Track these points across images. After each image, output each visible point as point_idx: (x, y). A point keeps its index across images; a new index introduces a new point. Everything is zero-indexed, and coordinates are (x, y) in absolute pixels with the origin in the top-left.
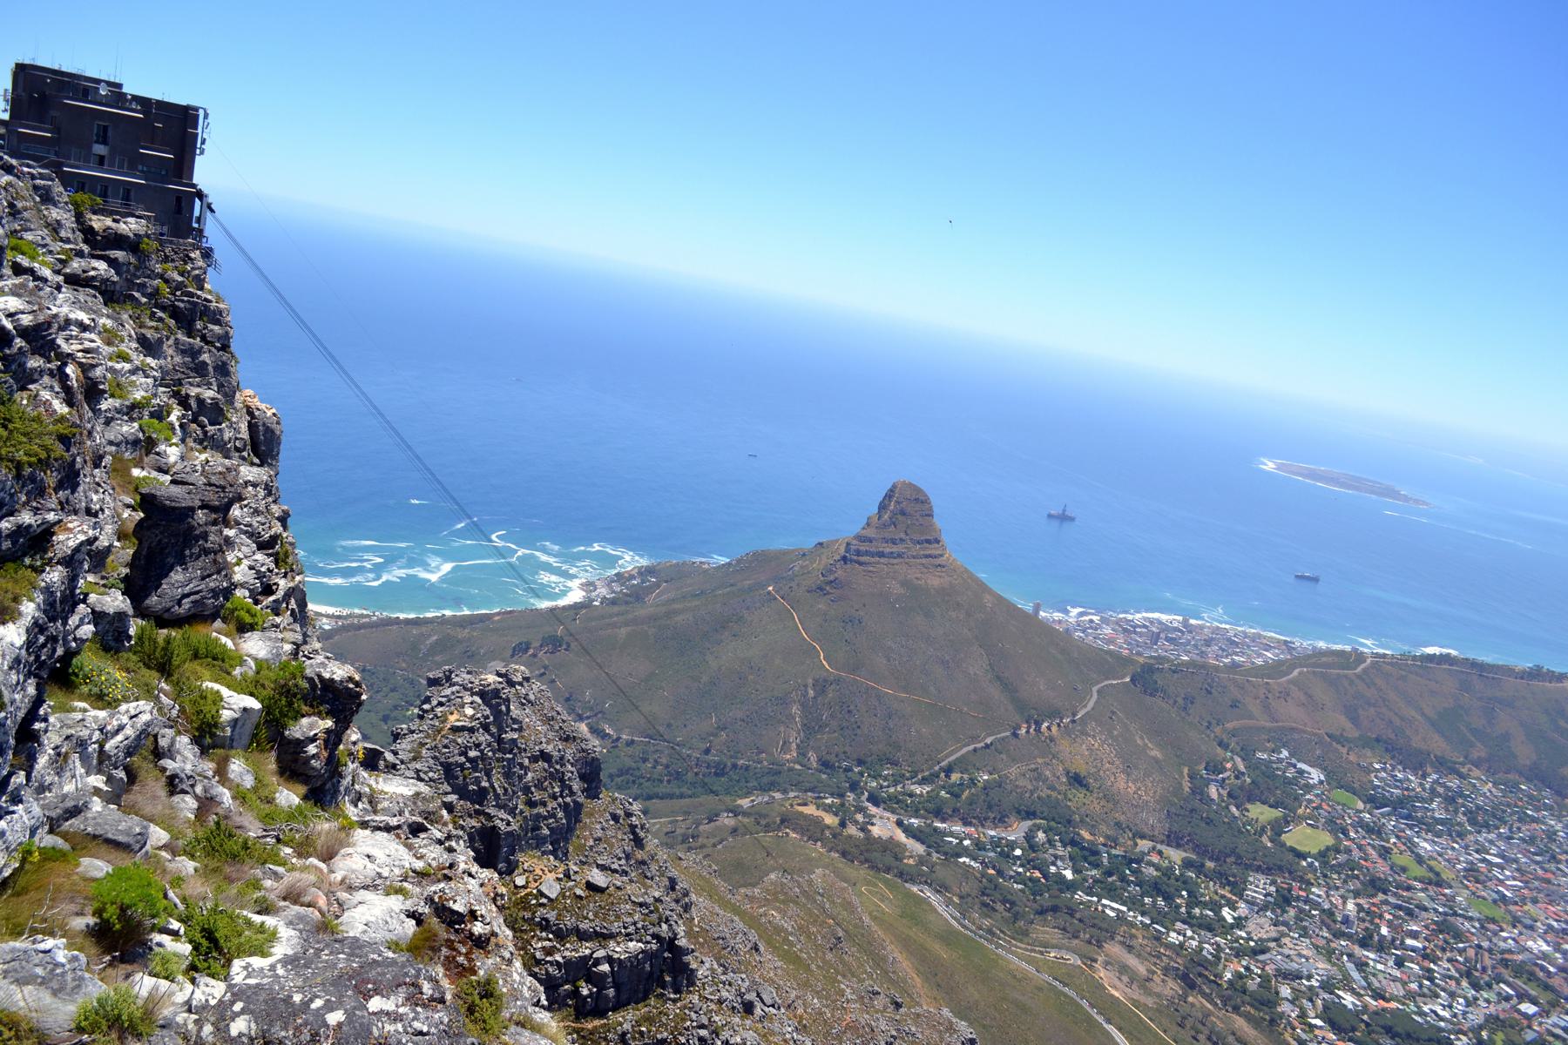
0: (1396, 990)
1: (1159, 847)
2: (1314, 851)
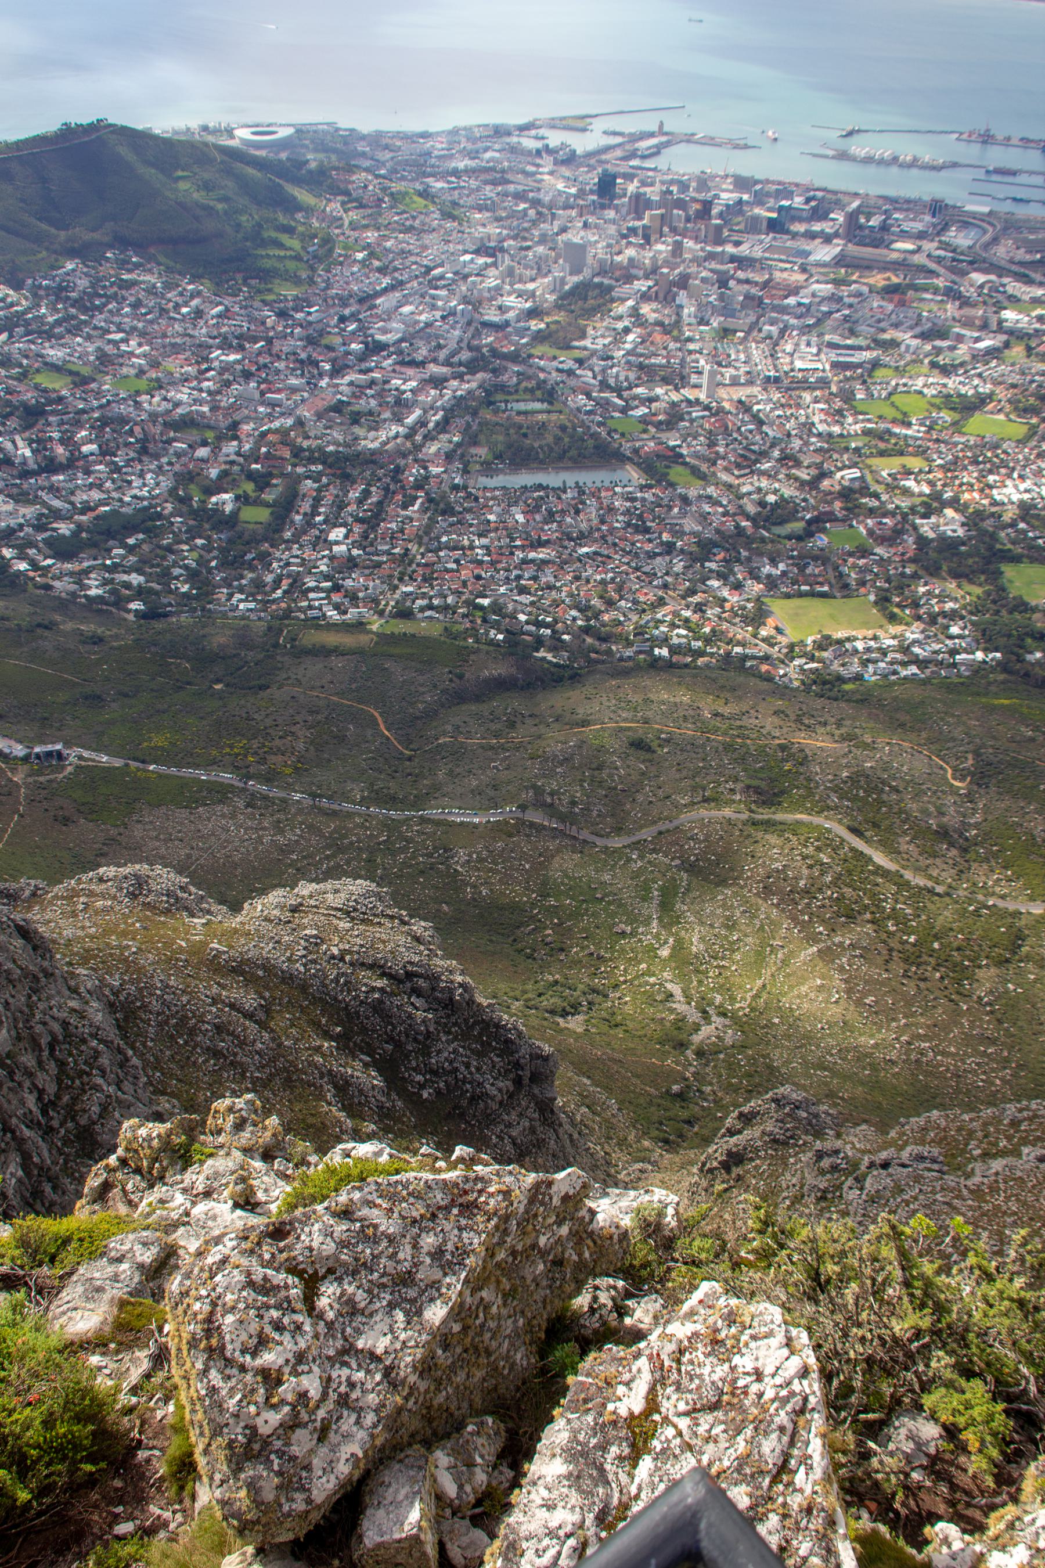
0: (96, 495)
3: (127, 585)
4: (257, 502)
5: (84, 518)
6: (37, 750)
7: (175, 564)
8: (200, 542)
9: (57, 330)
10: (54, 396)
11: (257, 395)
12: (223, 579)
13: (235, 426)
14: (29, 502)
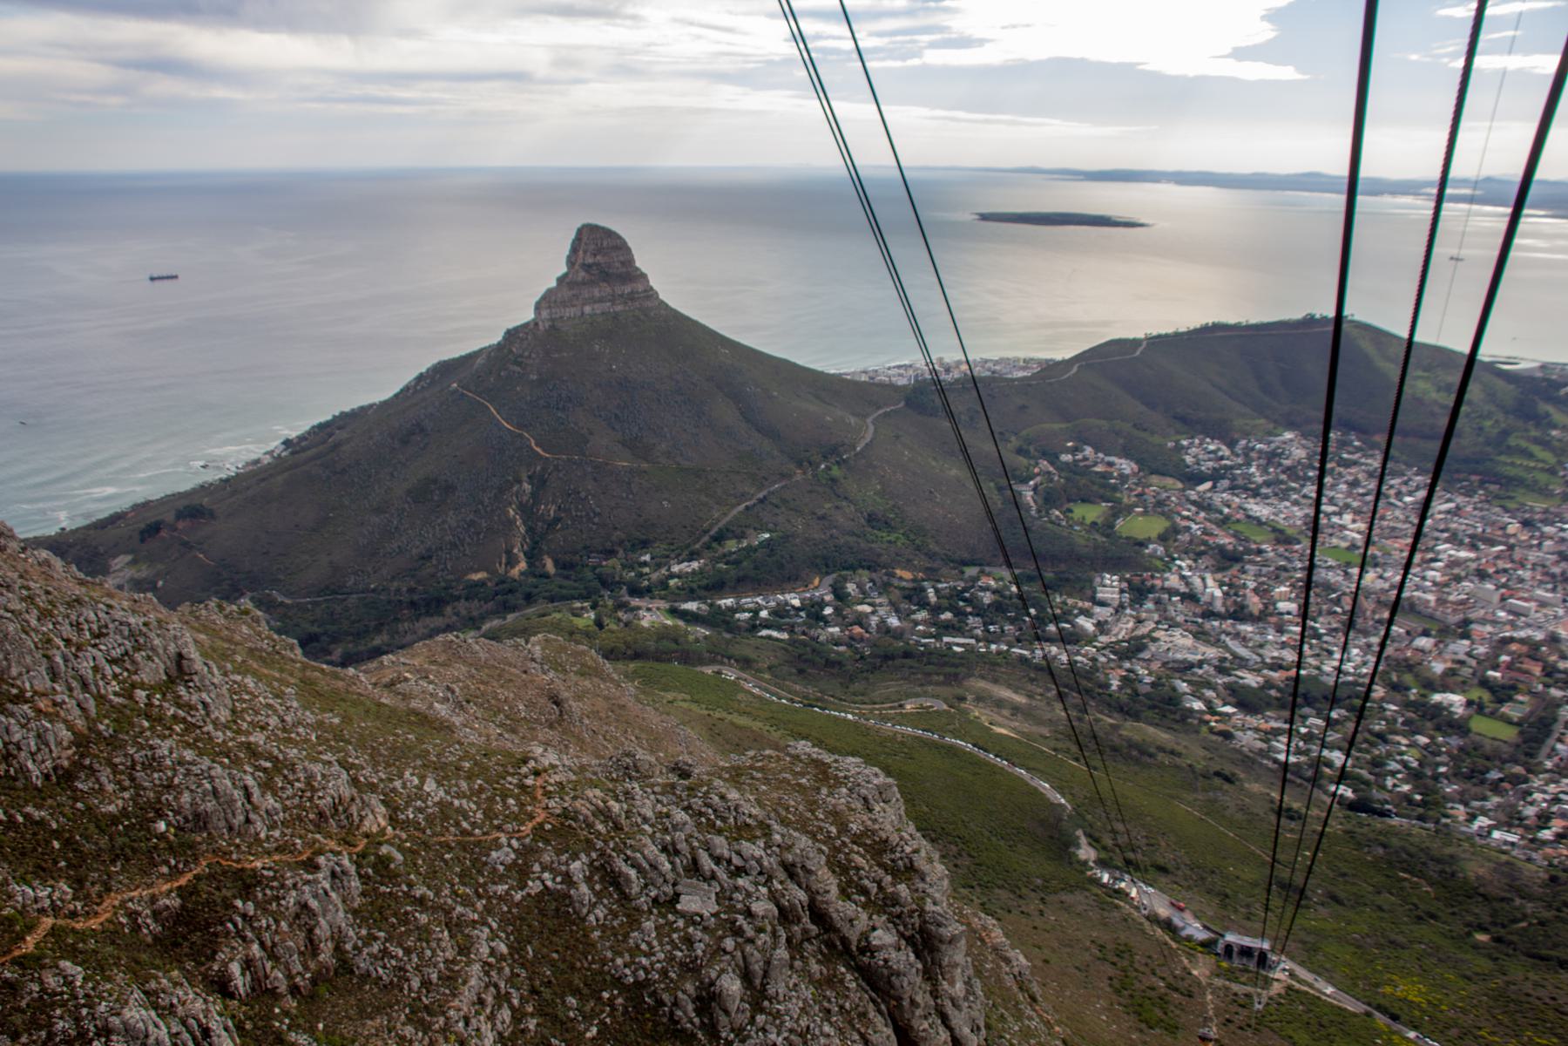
1: (987, 569)
2: (1154, 535)
3: (1329, 764)
4: (1493, 715)
5: (1275, 675)
6: (1230, 938)
7: (1389, 755)
8: (1423, 740)
9: (1264, 491)
10: (1254, 547)
11: (1496, 598)
12: (1462, 793)
13: (1466, 622)
14: (1207, 642)
